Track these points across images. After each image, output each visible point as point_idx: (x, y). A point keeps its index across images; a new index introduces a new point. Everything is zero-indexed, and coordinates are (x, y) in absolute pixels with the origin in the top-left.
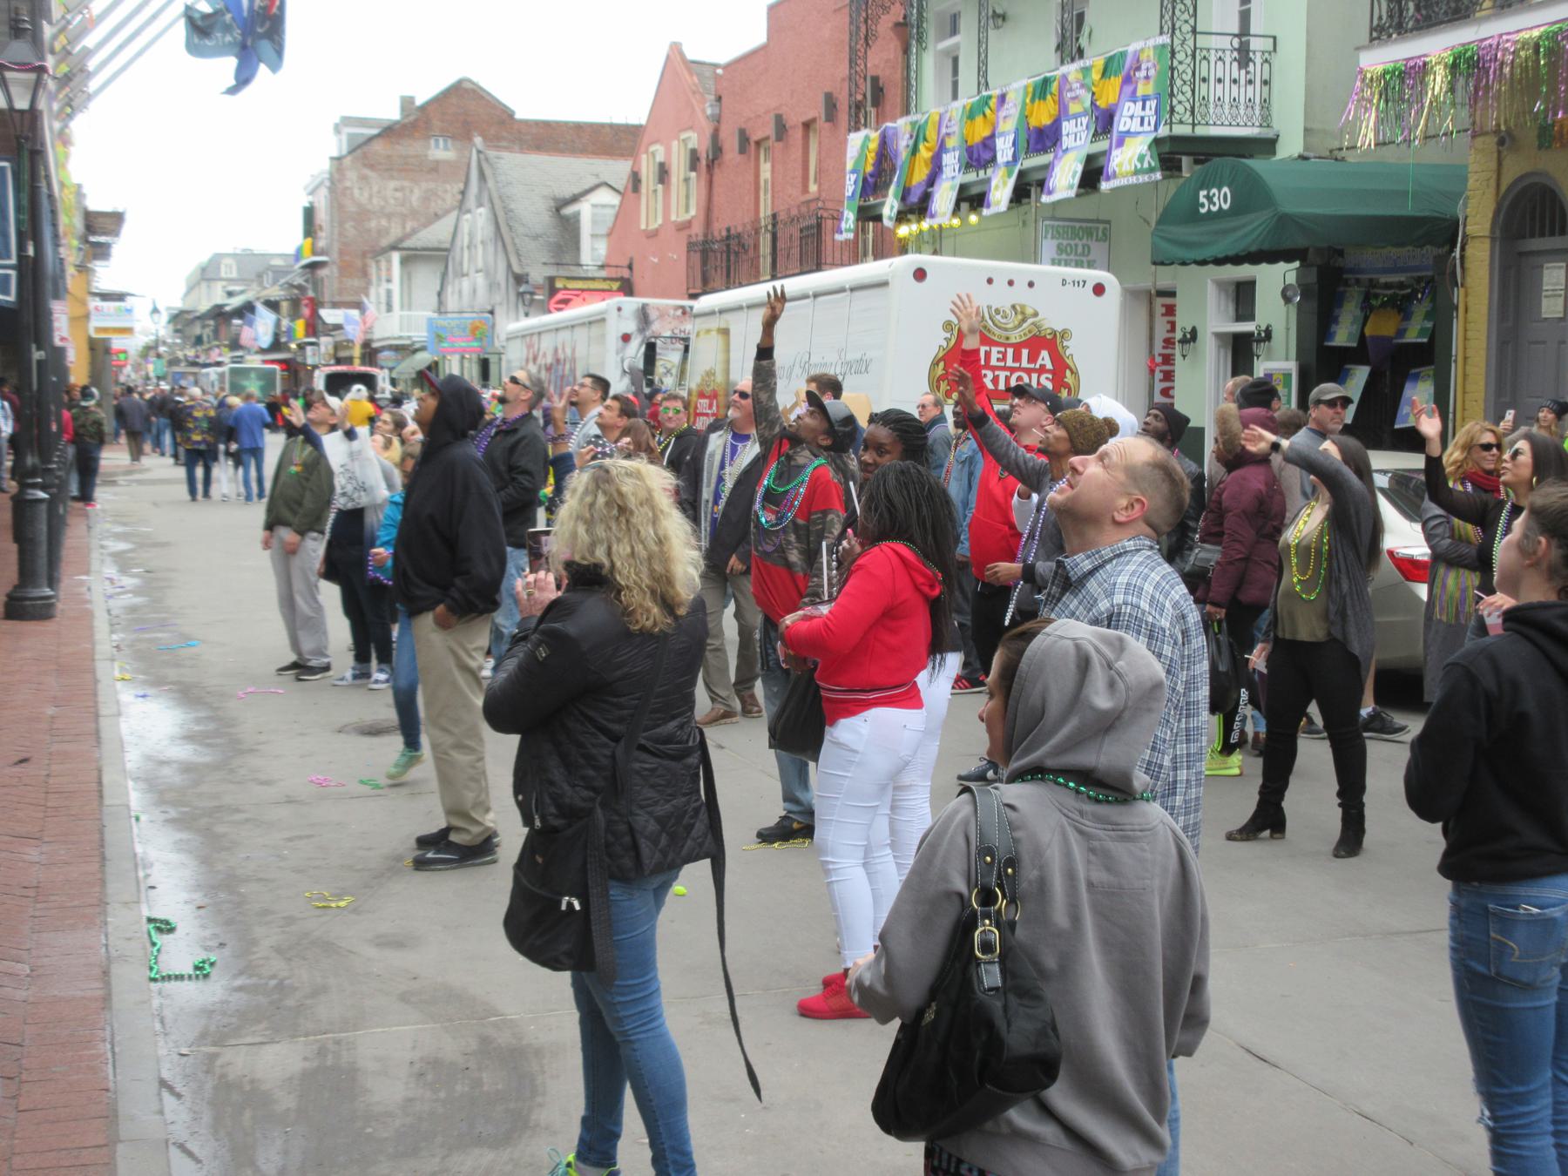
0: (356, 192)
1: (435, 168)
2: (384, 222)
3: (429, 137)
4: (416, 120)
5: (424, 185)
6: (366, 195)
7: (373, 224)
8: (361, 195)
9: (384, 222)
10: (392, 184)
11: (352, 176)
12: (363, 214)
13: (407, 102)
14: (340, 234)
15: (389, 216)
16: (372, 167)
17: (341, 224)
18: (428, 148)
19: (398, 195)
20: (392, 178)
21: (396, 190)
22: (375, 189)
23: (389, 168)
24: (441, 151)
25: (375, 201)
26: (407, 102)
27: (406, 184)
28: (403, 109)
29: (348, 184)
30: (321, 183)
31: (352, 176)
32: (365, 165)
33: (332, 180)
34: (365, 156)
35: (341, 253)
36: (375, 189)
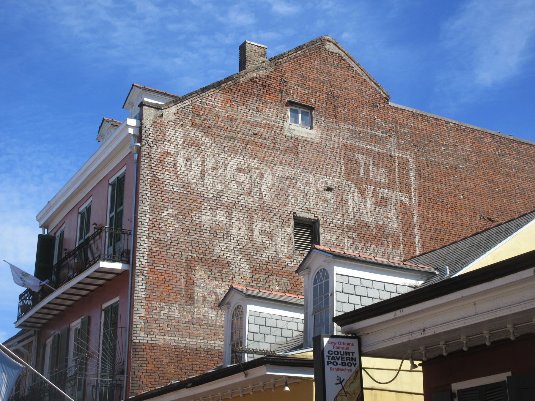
0: (181, 162)
1: (294, 147)
4: (268, 77)
5: (280, 171)
6: (196, 169)
7: (206, 217)
9: (221, 216)
10: (234, 162)
16: (207, 129)
18: (284, 119)
19: (243, 177)
20: (233, 150)
21: (239, 170)
22: (209, 164)
25: (208, 180)
27: (255, 163)
29: (171, 149)
32: (194, 125)
36: (209, 164)
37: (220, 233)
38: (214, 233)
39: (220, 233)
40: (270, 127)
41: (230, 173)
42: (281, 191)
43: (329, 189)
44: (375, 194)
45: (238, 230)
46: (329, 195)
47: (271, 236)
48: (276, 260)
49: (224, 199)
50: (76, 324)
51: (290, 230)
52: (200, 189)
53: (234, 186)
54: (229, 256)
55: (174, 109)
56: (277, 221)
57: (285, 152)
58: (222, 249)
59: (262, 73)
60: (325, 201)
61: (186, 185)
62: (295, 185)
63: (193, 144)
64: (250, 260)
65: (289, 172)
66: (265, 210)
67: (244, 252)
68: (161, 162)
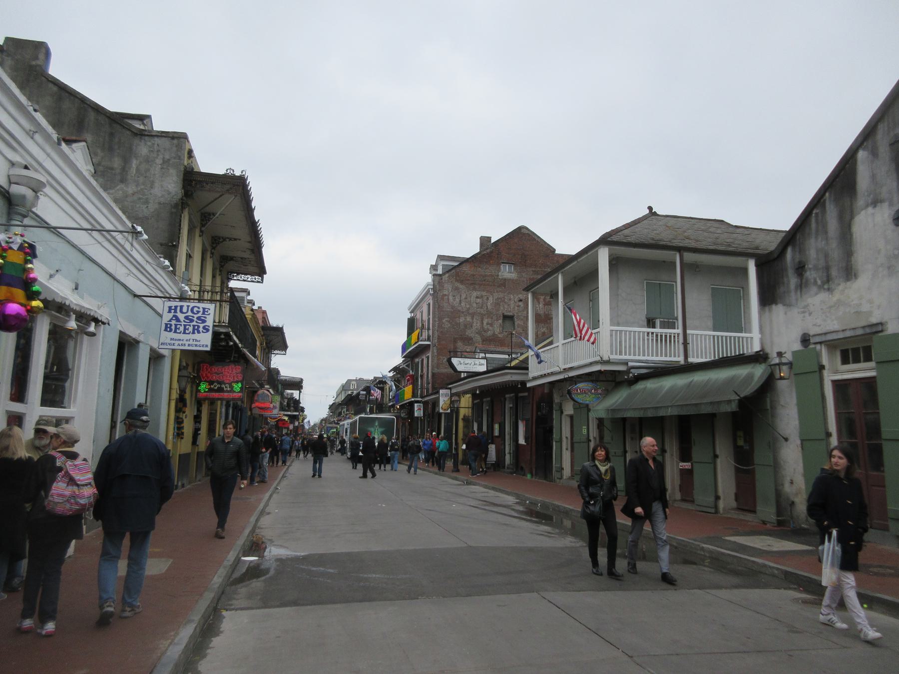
0: (451, 298)
1: (504, 284)
2: (469, 319)
3: (499, 264)
4: (492, 252)
5: (496, 295)
6: (457, 300)
8: (454, 300)
9: (469, 319)
10: (475, 294)
11: (448, 287)
12: (455, 313)
13: (484, 241)
14: (440, 326)
15: (473, 315)
16: (462, 282)
17: (440, 319)
18: (499, 270)
19: (478, 300)
20: (475, 289)
21: (477, 297)
22: (464, 296)
23: (472, 283)
24: (507, 272)
26: (484, 241)
27: (484, 293)
28: (482, 245)
29: (446, 292)
30: (428, 291)
31: (448, 287)
32: (457, 280)
33: (434, 289)
34: (457, 275)
35: (439, 338)
36: (464, 296)
37: (468, 326)
38: (465, 326)
39: (468, 326)
40: (492, 276)
41: (473, 299)
42: (497, 304)
43: (521, 300)
44: (544, 300)
45: (477, 325)
46: (520, 303)
47: (491, 325)
48: (494, 334)
49: (470, 311)
50: (424, 357)
51: (501, 321)
52: (460, 308)
53: (475, 305)
54: (472, 335)
55: (447, 275)
56: (494, 318)
57: (499, 286)
58: (470, 333)
59: (488, 251)
60: (518, 306)
61: (453, 307)
62: (504, 301)
63: (457, 289)
64: (482, 336)
65: (501, 295)
66: (489, 314)
67: (479, 333)
68: (442, 299)
